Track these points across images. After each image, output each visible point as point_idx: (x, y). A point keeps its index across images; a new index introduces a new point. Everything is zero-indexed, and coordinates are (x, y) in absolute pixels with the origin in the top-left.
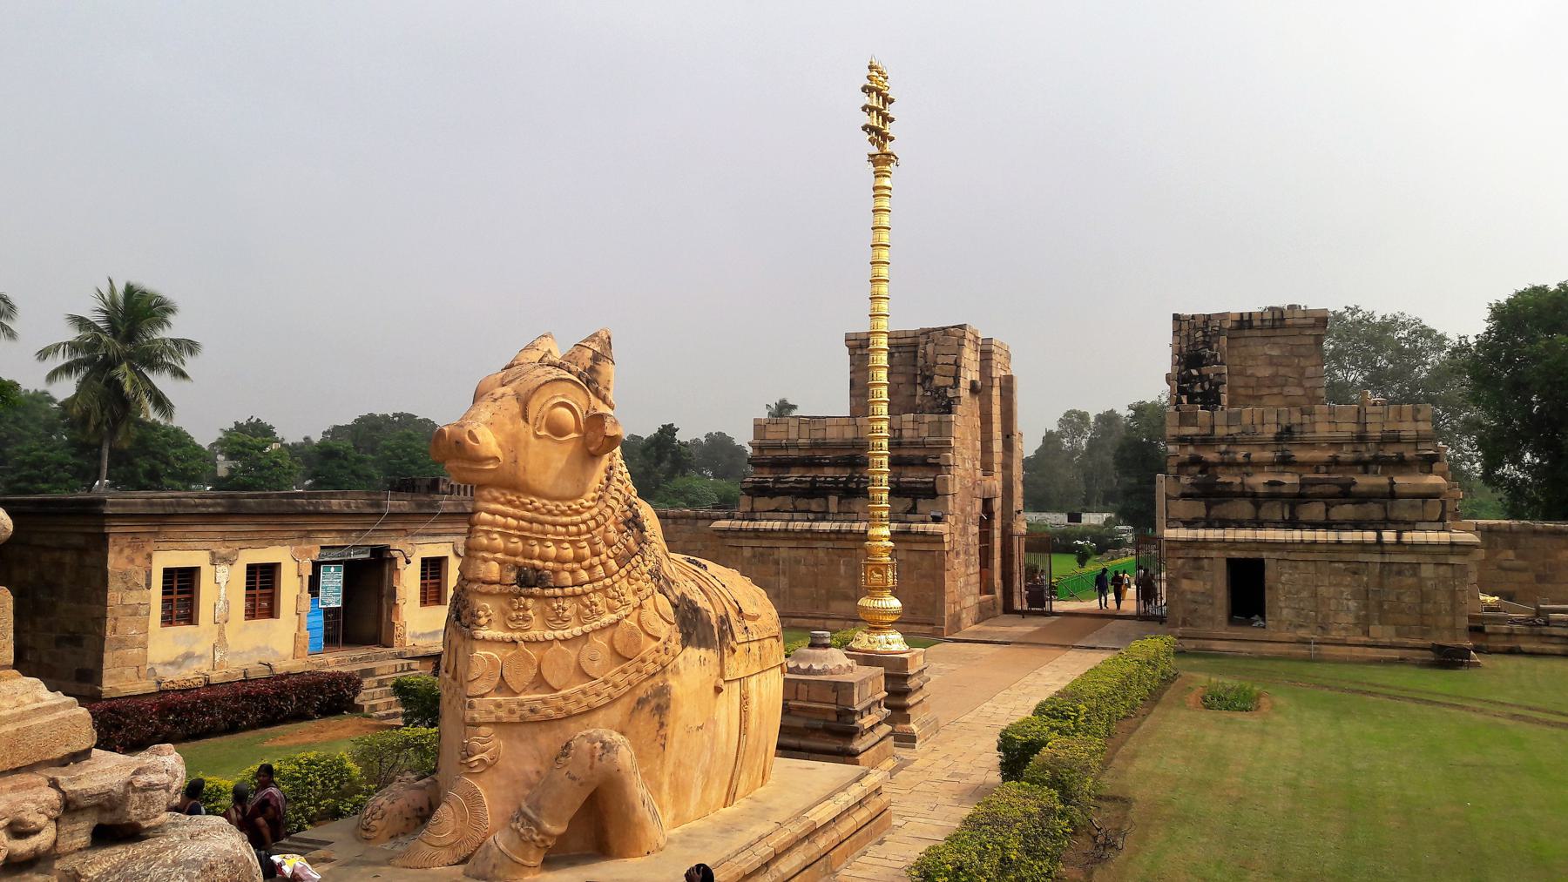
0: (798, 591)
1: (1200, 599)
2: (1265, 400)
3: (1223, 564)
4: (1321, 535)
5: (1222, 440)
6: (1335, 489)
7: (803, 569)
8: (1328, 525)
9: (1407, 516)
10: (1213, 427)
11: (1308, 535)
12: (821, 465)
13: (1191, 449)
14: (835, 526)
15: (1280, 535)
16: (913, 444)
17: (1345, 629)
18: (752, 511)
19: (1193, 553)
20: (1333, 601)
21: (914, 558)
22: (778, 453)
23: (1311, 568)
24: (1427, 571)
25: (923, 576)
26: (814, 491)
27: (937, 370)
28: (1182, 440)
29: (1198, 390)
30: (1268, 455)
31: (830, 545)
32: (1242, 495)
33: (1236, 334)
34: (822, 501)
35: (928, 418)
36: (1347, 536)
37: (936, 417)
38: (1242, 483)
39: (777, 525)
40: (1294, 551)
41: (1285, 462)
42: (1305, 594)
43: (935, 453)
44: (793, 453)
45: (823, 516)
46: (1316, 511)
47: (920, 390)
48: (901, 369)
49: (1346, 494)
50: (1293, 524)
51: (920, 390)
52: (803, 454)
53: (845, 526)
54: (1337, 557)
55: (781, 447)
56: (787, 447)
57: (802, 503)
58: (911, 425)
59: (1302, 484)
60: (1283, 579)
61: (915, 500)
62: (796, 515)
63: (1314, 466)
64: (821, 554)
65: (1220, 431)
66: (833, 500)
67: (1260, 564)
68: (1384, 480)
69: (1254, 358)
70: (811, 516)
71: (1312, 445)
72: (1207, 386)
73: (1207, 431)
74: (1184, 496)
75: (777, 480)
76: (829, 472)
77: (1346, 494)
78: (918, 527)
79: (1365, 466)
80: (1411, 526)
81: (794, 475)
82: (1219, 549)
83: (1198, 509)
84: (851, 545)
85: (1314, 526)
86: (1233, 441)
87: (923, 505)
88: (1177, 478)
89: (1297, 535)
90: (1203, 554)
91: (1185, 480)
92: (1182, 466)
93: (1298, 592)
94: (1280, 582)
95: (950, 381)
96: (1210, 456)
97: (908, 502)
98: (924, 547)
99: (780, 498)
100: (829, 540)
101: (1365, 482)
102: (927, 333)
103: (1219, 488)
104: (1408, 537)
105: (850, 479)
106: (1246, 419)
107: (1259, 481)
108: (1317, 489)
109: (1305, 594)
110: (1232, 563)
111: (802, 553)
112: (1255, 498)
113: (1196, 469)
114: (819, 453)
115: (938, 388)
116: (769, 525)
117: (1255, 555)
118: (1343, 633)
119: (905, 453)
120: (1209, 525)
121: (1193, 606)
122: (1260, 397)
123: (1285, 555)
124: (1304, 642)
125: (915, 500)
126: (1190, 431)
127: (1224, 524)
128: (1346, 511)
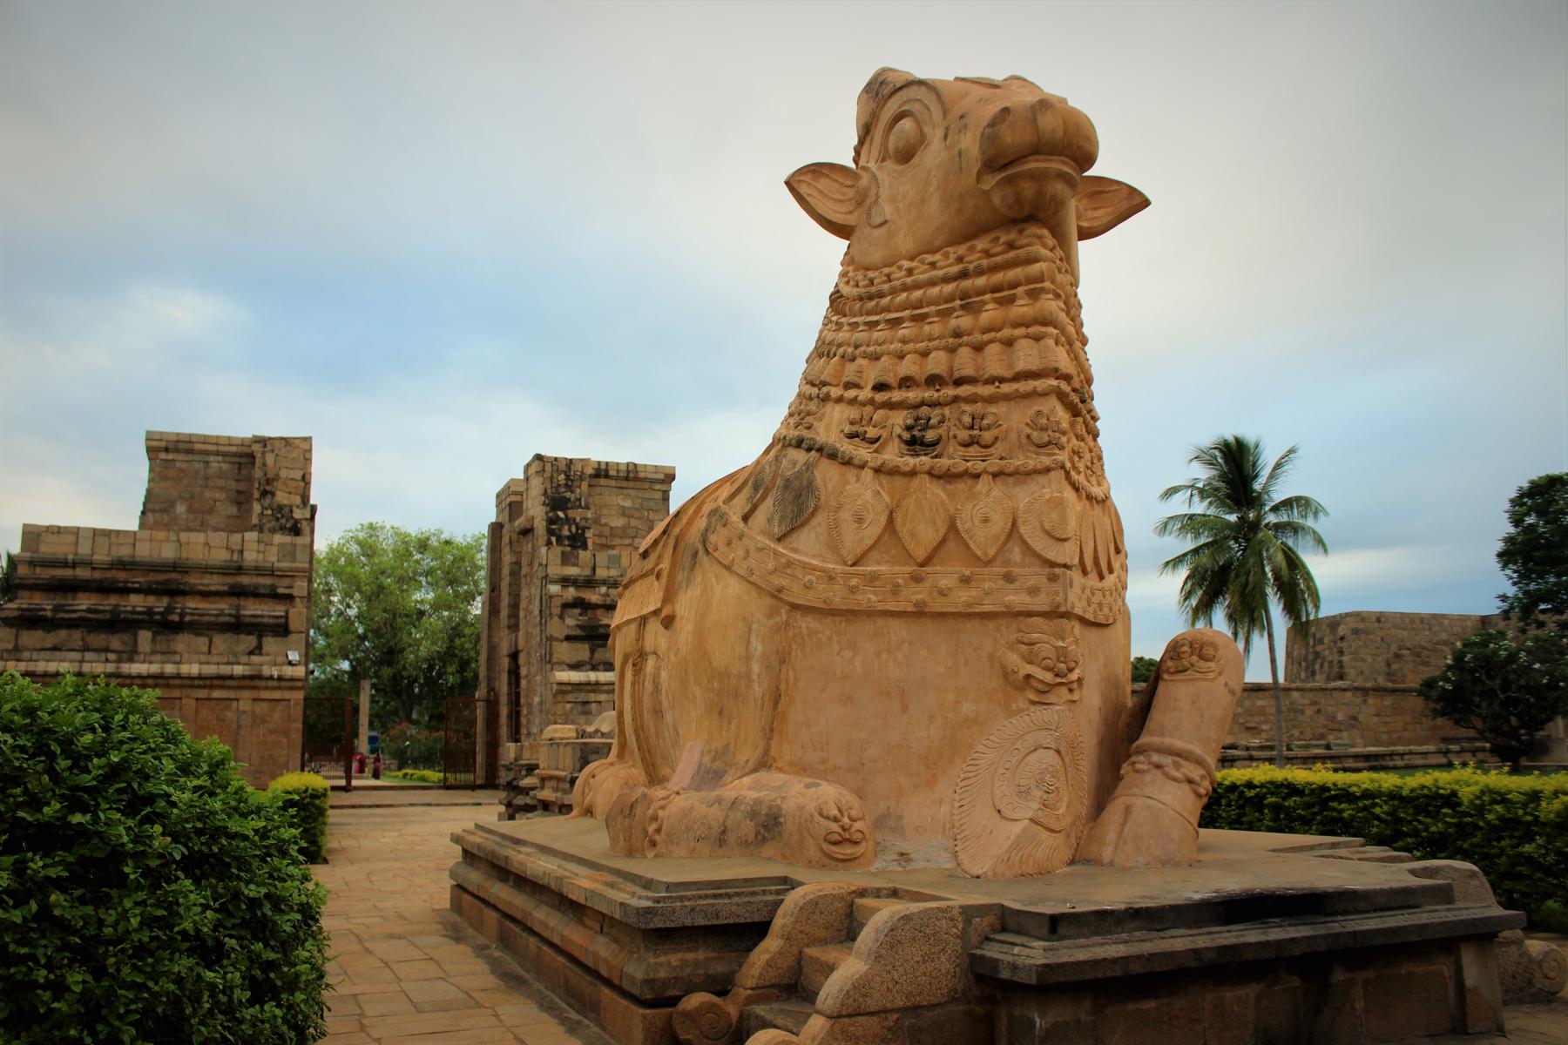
5: (604, 582)
10: (594, 569)
12: (126, 591)
13: (572, 590)
14: (154, 668)
16: (258, 571)
18: (16, 649)
19: (582, 697)
21: (261, 708)
25: (272, 732)
26: (116, 624)
27: (278, 484)
28: (565, 581)
29: (566, 532)
33: (595, 481)
34: (126, 637)
35: (279, 538)
37: (288, 539)
43: (286, 582)
44: (83, 573)
45: (131, 655)
47: (257, 508)
48: (221, 483)
52: (97, 575)
53: (170, 669)
55: (65, 564)
56: (74, 565)
57: (99, 639)
61: (260, 638)
62: (88, 656)
65: (601, 573)
70: (112, 656)
72: (574, 529)
73: (587, 572)
74: (569, 638)
75: (58, 609)
76: (137, 602)
78: (266, 671)
83: (582, 651)
84: (177, 693)
87: (270, 643)
88: (561, 617)
90: (592, 697)
91: (570, 622)
92: (566, 606)
95: (297, 500)
96: (593, 597)
97: (250, 641)
98: (277, 695)
99: (63, 633)
102: (263, 441)
105: (169, 610)
106: (625, 562)
113: (577, 611)
114: (122, 576)
115: (280, 508)
119: (245, 580)
120: (594, 668)
125: (260, 638)
126: (572, 571)
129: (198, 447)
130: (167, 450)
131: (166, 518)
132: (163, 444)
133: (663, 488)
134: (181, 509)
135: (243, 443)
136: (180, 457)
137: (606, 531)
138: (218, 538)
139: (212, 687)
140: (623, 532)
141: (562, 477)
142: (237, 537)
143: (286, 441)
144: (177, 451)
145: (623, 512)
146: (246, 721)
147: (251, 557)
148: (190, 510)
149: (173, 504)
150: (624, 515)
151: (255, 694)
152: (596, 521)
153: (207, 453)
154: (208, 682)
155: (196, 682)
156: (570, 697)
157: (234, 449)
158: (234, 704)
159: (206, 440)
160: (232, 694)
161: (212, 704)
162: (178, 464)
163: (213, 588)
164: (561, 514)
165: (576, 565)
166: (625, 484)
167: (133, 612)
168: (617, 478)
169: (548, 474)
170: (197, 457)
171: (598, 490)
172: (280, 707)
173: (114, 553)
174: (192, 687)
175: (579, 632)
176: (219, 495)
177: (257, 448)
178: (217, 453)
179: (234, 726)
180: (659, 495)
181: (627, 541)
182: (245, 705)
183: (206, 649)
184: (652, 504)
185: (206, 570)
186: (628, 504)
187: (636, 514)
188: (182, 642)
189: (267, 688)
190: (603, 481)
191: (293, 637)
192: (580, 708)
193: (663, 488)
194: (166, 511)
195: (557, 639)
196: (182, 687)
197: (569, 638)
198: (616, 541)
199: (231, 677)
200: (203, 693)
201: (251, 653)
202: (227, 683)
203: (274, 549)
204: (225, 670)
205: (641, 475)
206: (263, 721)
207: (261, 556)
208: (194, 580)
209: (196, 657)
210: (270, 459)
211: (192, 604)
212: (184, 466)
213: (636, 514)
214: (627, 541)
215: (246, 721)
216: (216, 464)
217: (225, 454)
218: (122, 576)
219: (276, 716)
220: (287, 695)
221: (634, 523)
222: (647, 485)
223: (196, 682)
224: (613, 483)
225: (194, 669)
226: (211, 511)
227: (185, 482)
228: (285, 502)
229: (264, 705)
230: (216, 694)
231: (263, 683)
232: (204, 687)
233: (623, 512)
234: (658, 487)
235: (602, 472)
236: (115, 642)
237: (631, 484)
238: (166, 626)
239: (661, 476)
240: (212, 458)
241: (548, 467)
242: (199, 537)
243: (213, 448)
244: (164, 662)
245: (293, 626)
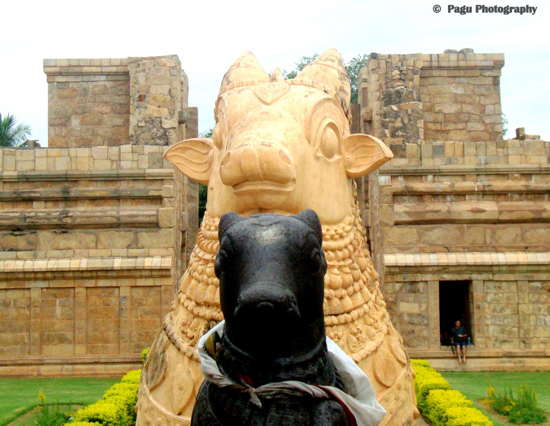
1: (416, 320)
2: (451, 134)
3: (436, 287)
6: (531, 216)
12: (30, 200)
13: (401, 179)
17: (542, 342)
19: (410, 277)
20: (533, 318)
21: (138, 294)
23: (513, 287)
25: (147, 313)
31: (44, 284)
33: (427, 73)
35: (149, 149)
37: (155, 149)
38: (449, 212)
40: (499, 272)
42: (508, 312)
43: (156, 186)
48: (106, 98)
54: (537, 276)
58: (130, 156)
59: (500, 212)
60: (489, 298)
61: (136, 233)
64: (35, 295)
65: (428, 164)
67: (467, 284)
69: (439, 93)
72: (406, 121)
74: (397, 224)
82: (434, 273)
84: (71, 284)
86: (438, 174)
90: (419, 277)
93: (502, 310)
95: (165, 111)
98: (150, 282)
100: (45, 279)
102: (136, 62)
103: (429, 216)
108: (514, 216)
109: (508, 312)
110: (444, 286)
117: (466, 277)
118: (542, 346)
120: (422, 251)
121: (410, 327)
122: (447, 132)
123: (490, 276)
124: (510, 356)
129: (85, 69)
130: (60, 74)
131: (64, 131)
132: (57, 69)
133: (494, 73)
134: (75, 122)
135: (123, 64)
136: (71, 79)
137: (440, 117)
138: (100, 151)
139: (98, 278)
140: (457, 118)
141: (396, 72)
142: (115, 149)
144: (68, 74)
145: (456, 99)
146: (127, 304)
147: (127, 166)
148: (83, 123)
149: (69, 119)
150: (456, 101)
151: (132, 282)
152: (430, 109)
153: (95, 74)
154: (94, 274)
155: (85, 275)
156: (399, 278)
157: (114, 69)
158: (117, 290)
159: (91, 63)
160: (114, 283)
161: (99, 291)
162: (71, 85)
163: (98, 194)
164: (395, 108)
165: (403, 157)
166: (456, 73)
167: (36, 217)
168: (449, 68)
169: (382, 71)
170: (86, 78)
171: (431, 80)
172: (153, 292)
173: (19, 169)
174: (83, 278)
175: (407, 218)
176: (106, 109)
177: (131, 69)
178: (101, 74)
179: (117, 309)
180: (490, 81)
181: (460, 126)
182: (125, 292)
183: (93, 245)
184: (483, 91)
185: (92, 179)
186: (460, 91)
187: (468, 100)
189: (141, 277)
190: (435, 73)
191: (162, 232)
192: (408, 287)
193: (494, 73)
194: (64, 125)
195: (387, 225)
196: (74, 278)
197: (397, 224)
198: (451, 126)
199: (112, 270)
200: (91, 283)
201: (129, 247)
202: (109, 274)
203: (146, 158)
204: (106, 264)
205: (472, 64)
206: (140, 304)
207: (135, 164)
209: (85, 252)
212: (75, 86)
213: (468, 100)
214: (460, 126)
215: (127, 304)
216: (102, 81)
217: (108, 74)
219: (150, 300)
220: (158, 282)
221: (467, 108)
222: (478, 73)
223: (85, 275)
224: (445, 73)
225: (83, 263)
226: (99, 123)
227: (78, 99)
228: (156, 115)
229: (141, 291)
230: (102, 283)
231: (138, 274)
232: (92, 278)
234: (488, 73)
236: (21, 241)
237: (462, 73)
238: (63, 228)
239: (491, 63)
240: (97, 78)
241: (383, 64)
242: (84, 152)
243: (99, 70)
244: (58, 258)
245: (161, 224)
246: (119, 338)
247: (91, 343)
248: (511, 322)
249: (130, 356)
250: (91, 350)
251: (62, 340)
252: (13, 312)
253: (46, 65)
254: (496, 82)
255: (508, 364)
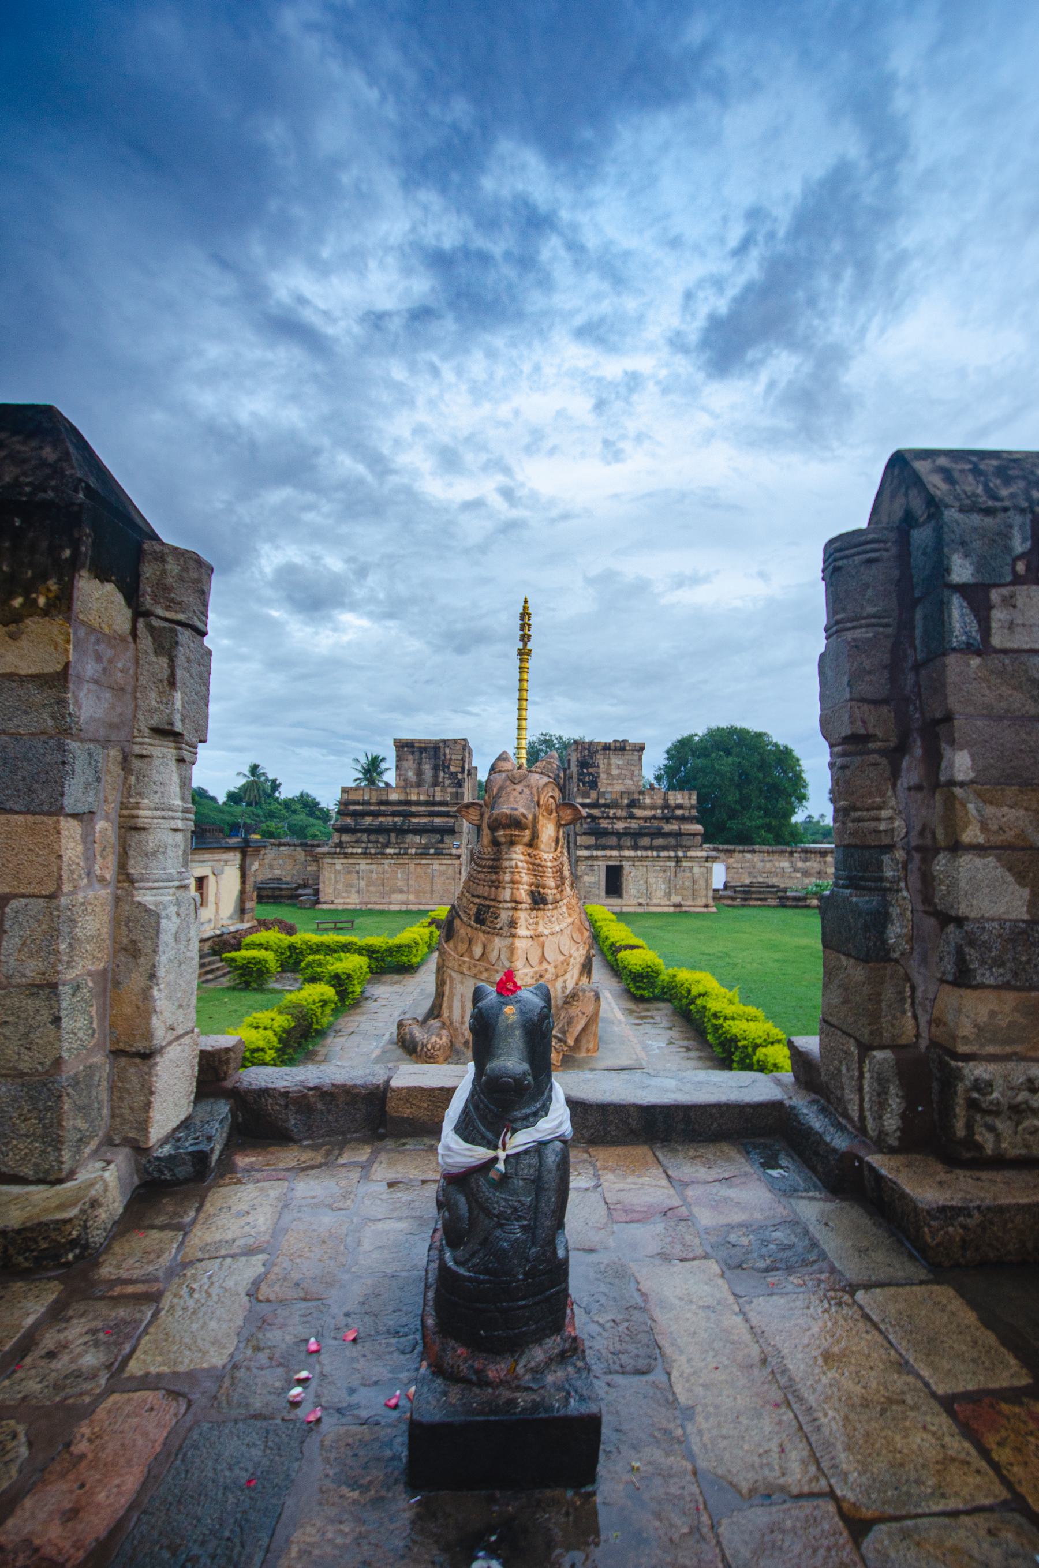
0: (372, 889)
4: (649, 853)
7: (374, 876)
8: (651, 848)
9: (689, 843)
11: (645, 854)
14: (397, 851)
15: (632, 853)
22: (357, 807)
24: (696, 870)
28: (584, 805)
30: (624, 814)
32: (612, 833)
35: (449, 790)
36: (663, 854)
39: (359, 851)
41: (632, 817)
45: (387, 845)
46: (645, 841)
47: (442, 774)
49: (659, 833)
50: (635, 847)
51: (442, 774)
57: (373, 837)
63: (646, 819)
66: (393, 836)
68: (676, 827)
71: (644, 807)
76: (390, 819)
77: (659, 833)
79: (667, 819)
80: (689, 848)
81: (368, 820)
83: (591, 840)
85: (646, 848)
87: (447, 839)
89: (639, 853)
94: (633, 878)
96: (596, 812)
97: (438, 837)
101: (668, 828)
102: (444, 741)
104: (689, 854)
107: (620, 826)
111: (374, 866)
112: (618, 835)
115: (452, 773)
116: (354, 851)
126: (588, 801)
127: (604, 848)
128: (659, 841)
135: (437, 742)
143: (455, 741)
145: (618, 767)
146: (436, 874)
147: (438, 799)
182: (436, 867)
188: (409, 838)
208: (414, 809)
210: (447, 751)
211: (415, 820)
218: (383, 808)
230: (424, 862)
233: (618, 767)
235: (606, 747)
246: (432, 891)
247: (417, 893)
248: (644, 887)
249: (438, 900)
250: (417, 897)
251: (401, 892)
252: (374, 876)
253: (396, 741)
254: (640, 759)
255: (640, 910)
